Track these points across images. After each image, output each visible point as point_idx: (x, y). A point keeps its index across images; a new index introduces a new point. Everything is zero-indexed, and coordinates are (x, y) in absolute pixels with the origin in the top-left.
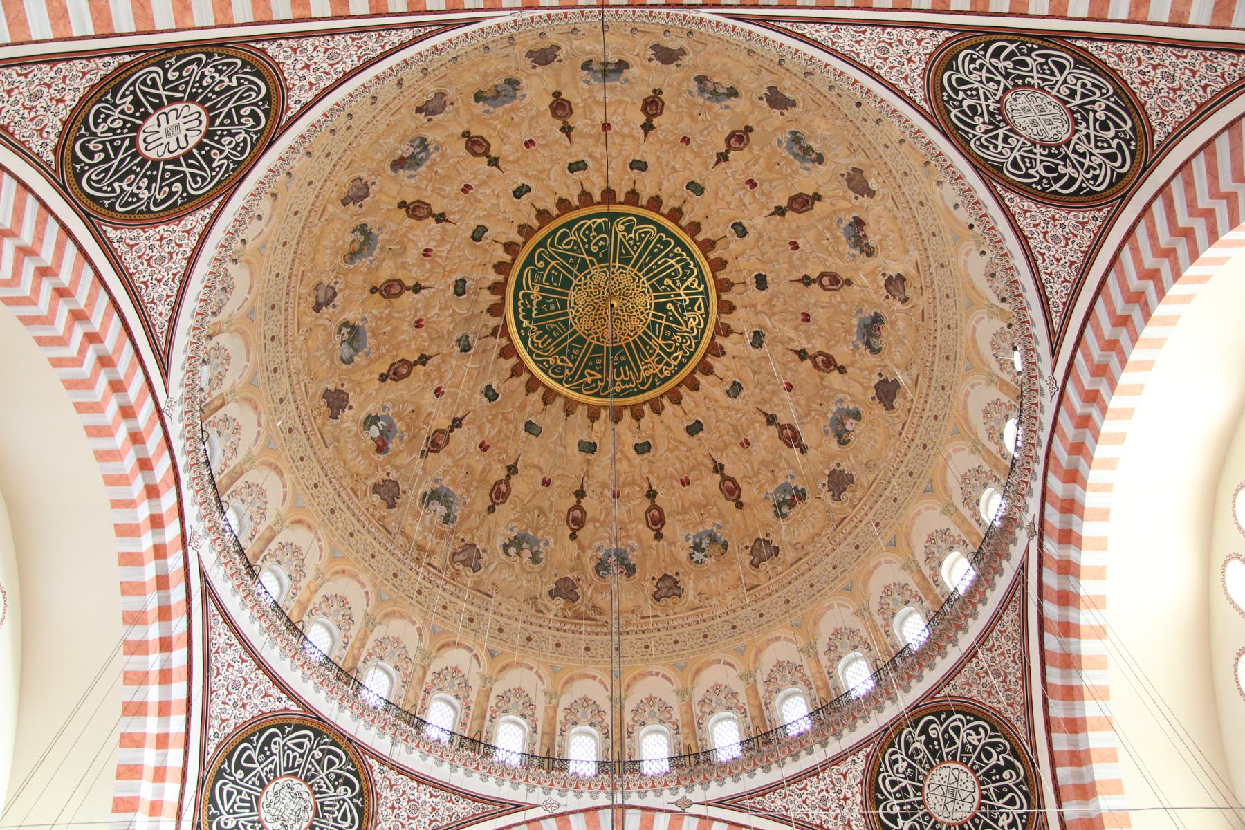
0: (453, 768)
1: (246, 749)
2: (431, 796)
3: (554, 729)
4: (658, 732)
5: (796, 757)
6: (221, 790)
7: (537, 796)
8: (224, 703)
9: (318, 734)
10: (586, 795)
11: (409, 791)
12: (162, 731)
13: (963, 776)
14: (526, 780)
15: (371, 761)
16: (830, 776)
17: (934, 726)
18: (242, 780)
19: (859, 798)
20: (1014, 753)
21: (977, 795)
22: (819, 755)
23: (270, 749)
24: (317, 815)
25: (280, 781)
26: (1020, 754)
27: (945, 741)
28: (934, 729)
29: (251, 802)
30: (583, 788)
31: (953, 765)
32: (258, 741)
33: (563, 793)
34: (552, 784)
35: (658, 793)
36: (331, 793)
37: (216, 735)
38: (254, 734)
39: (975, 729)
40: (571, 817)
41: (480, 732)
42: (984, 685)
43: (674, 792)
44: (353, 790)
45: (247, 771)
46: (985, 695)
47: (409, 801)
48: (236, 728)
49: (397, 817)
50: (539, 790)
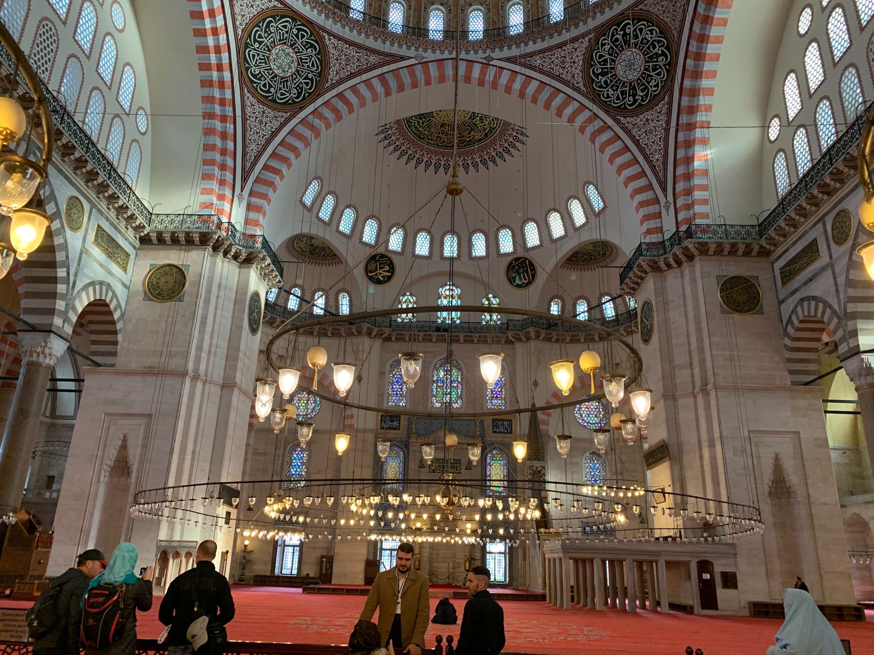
0: (367, 36)
1: (257, 31)
2: (357, 52)
3: (421, 7)
4: (478, 10)
5: (551, 36)
6: (249, 54)
7: (412, 52)
8: (241, 5)
9: (294, 20)
10: (438, 51)
11: (344, 50)
12: (214, 26)
13: (638, 57)
14: (406, 43)
15: (324, 34)
16: (568, 49)
18: (258, 48)
19: (581, 62)
20: (667, 48)
21: (642, 68)
22: (566, 36)
23: (270, 30)
24: (299, 64)
25: (278, 47)
26: (672, 48)
27: (634, 35)
28: (629, 28)
29: (265, 59)
30: (436, 48)
31: (634, 50)
32: (263, 25)
33: (425, 50)
34: (420, 45)
35: (476, 52)
36: (305, 52)
37: (241, 25)
38: (260, 22)
40: (430, 64)
41: (380, 11)
42: (662, 6)
43: (484, 51)
44: (316, 51)
45: (260, 43)
46: (662, 12)
47: (345, 55)
48: (250, 20)
49: (340, 64)
50: (413, 48)
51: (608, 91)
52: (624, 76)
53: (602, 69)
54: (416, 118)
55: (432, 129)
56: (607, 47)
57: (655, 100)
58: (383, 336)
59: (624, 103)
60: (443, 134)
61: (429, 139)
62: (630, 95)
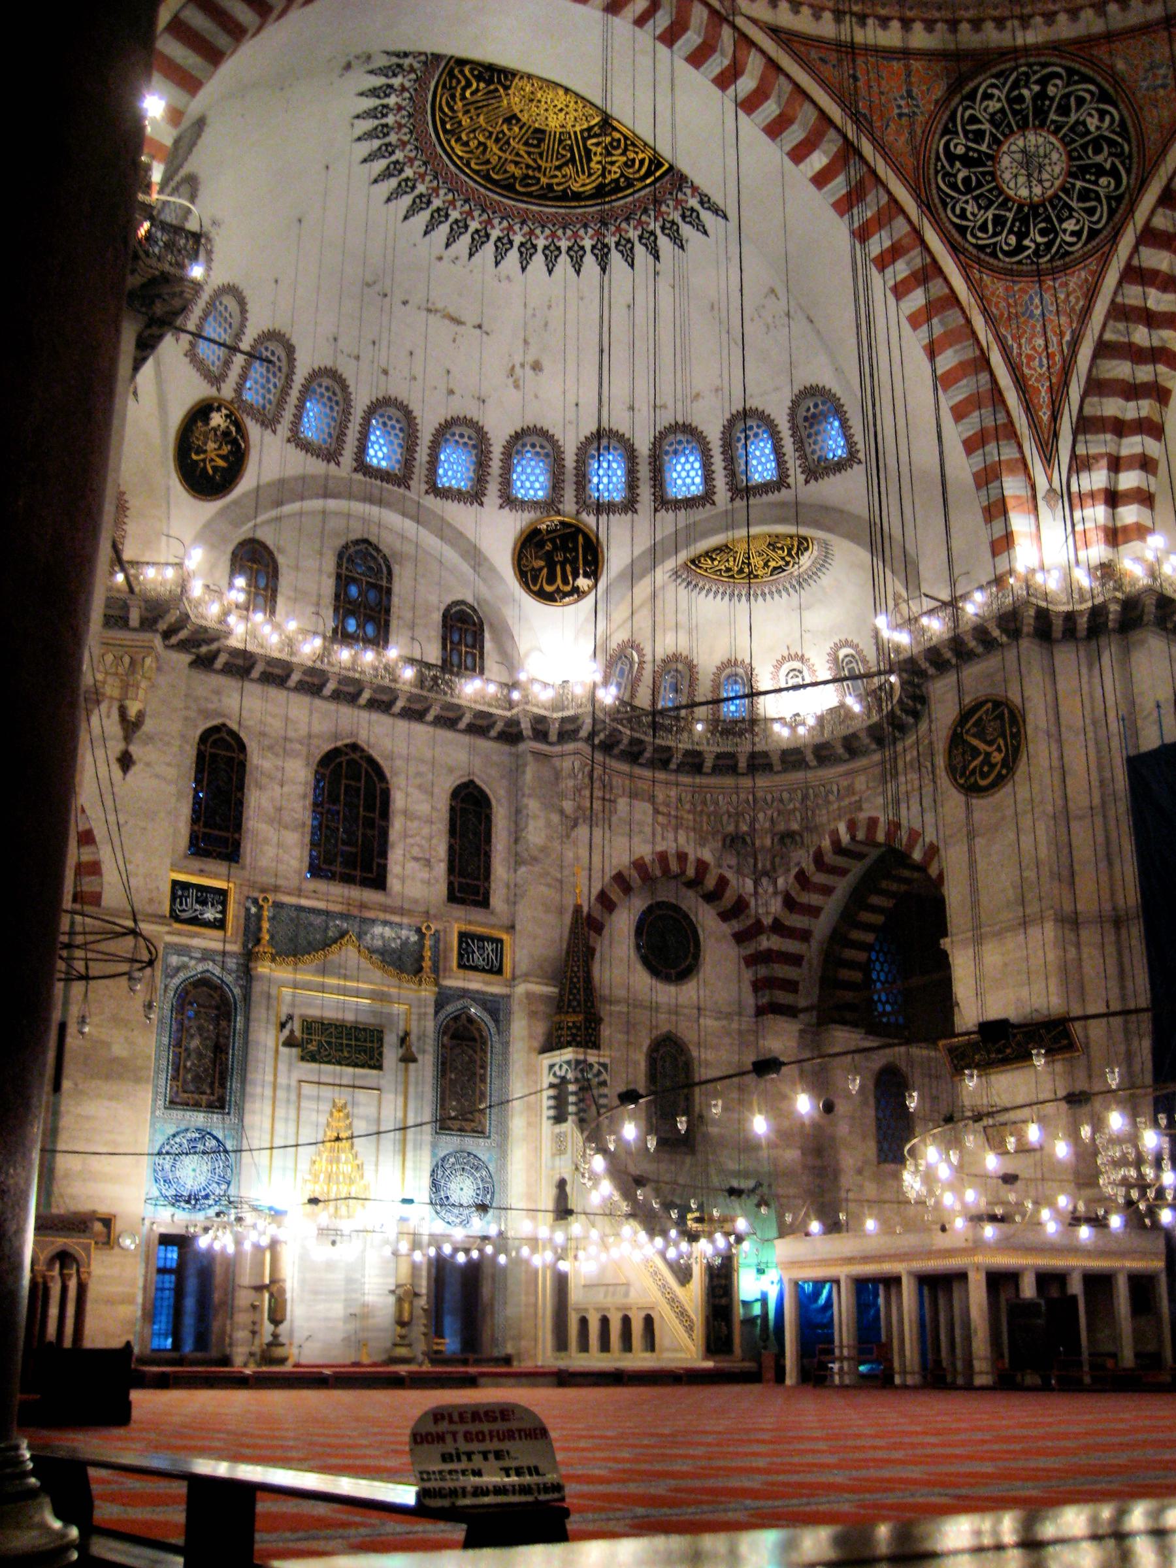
13: (1055, 156)
17: (1058, 82)
21: (1057, 183)
28: (1056, 85)
31: (1052, 139)
39: (1102, 114)
51: (967, 202)
52: (1012, 185)
53: (968, 149)
54: (471, 71)
55: (482, 118)
56: (994, 105)
57: (1063, 263)
58: (204, 649)
59: (995, 244)
60: (497, 140)
61: (458, 140)
62: (1011, 232)
